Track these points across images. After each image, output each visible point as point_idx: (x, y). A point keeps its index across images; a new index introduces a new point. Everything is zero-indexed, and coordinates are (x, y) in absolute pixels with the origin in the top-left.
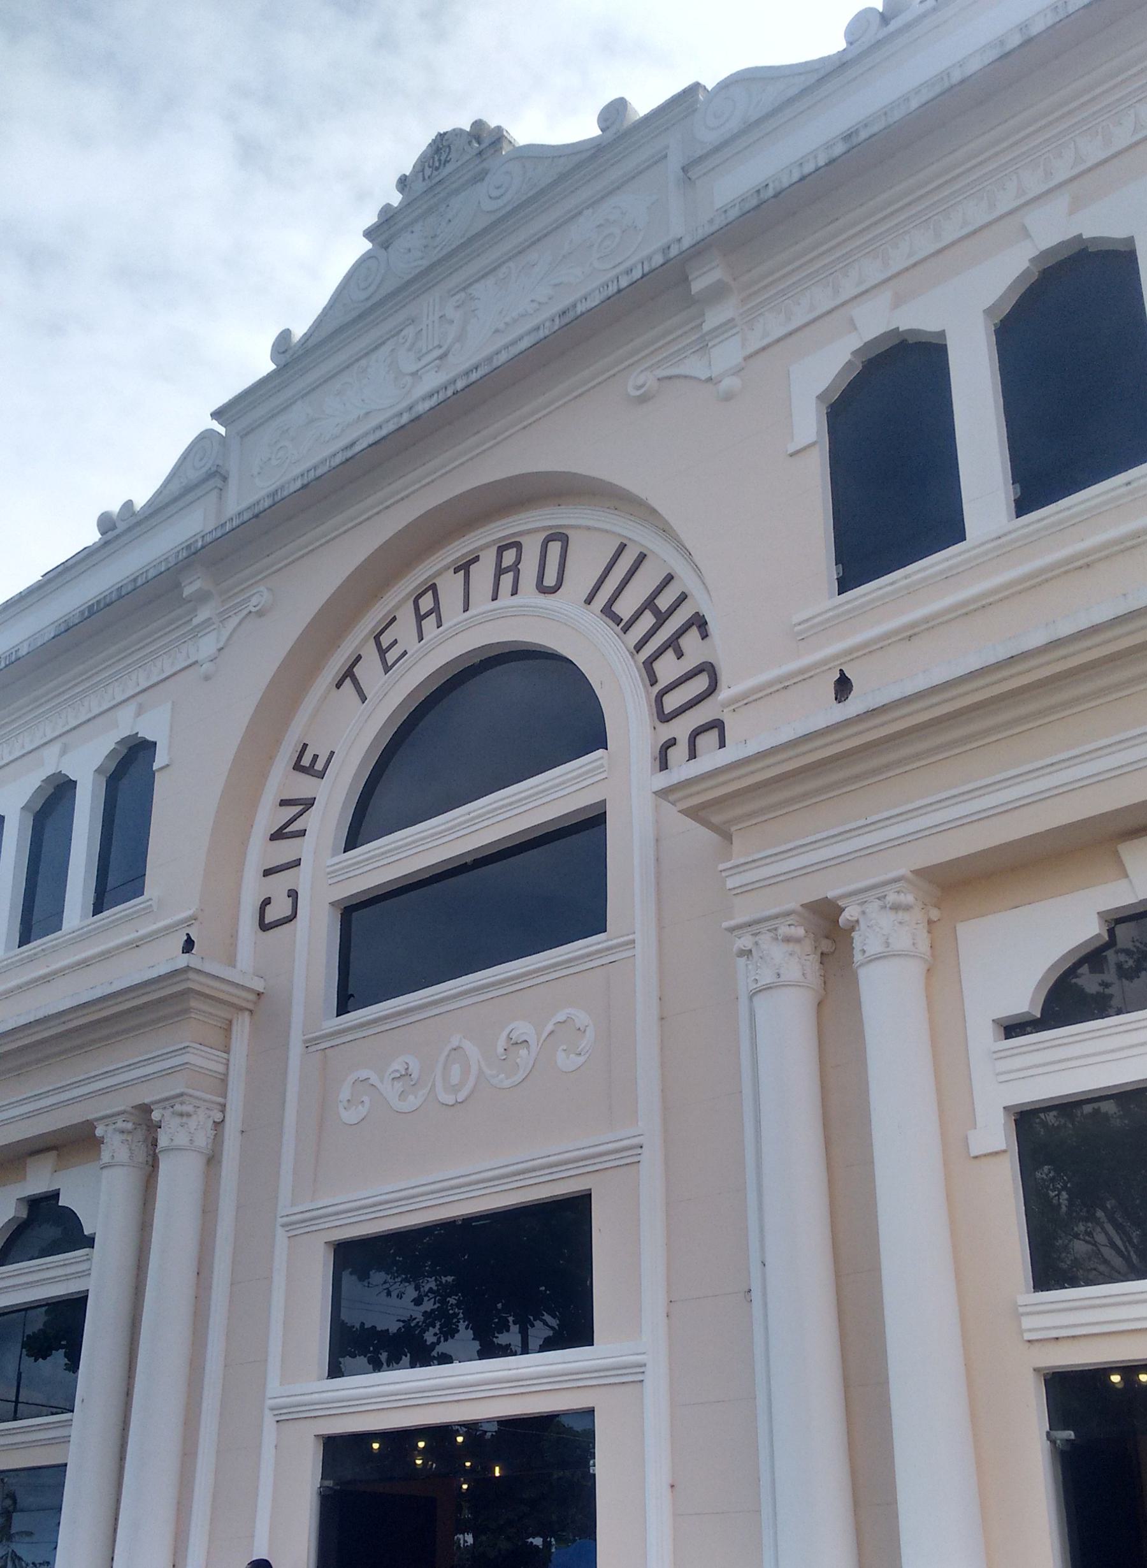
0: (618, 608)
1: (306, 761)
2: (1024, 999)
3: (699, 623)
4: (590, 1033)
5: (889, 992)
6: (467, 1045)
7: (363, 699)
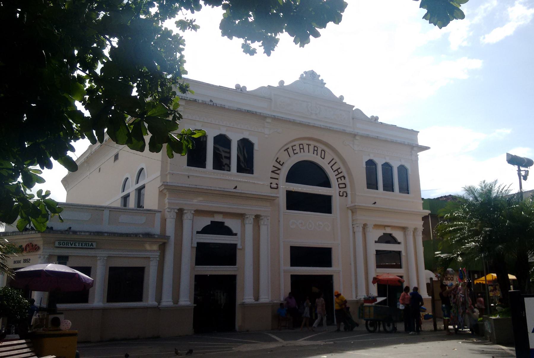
3: (344, 178)
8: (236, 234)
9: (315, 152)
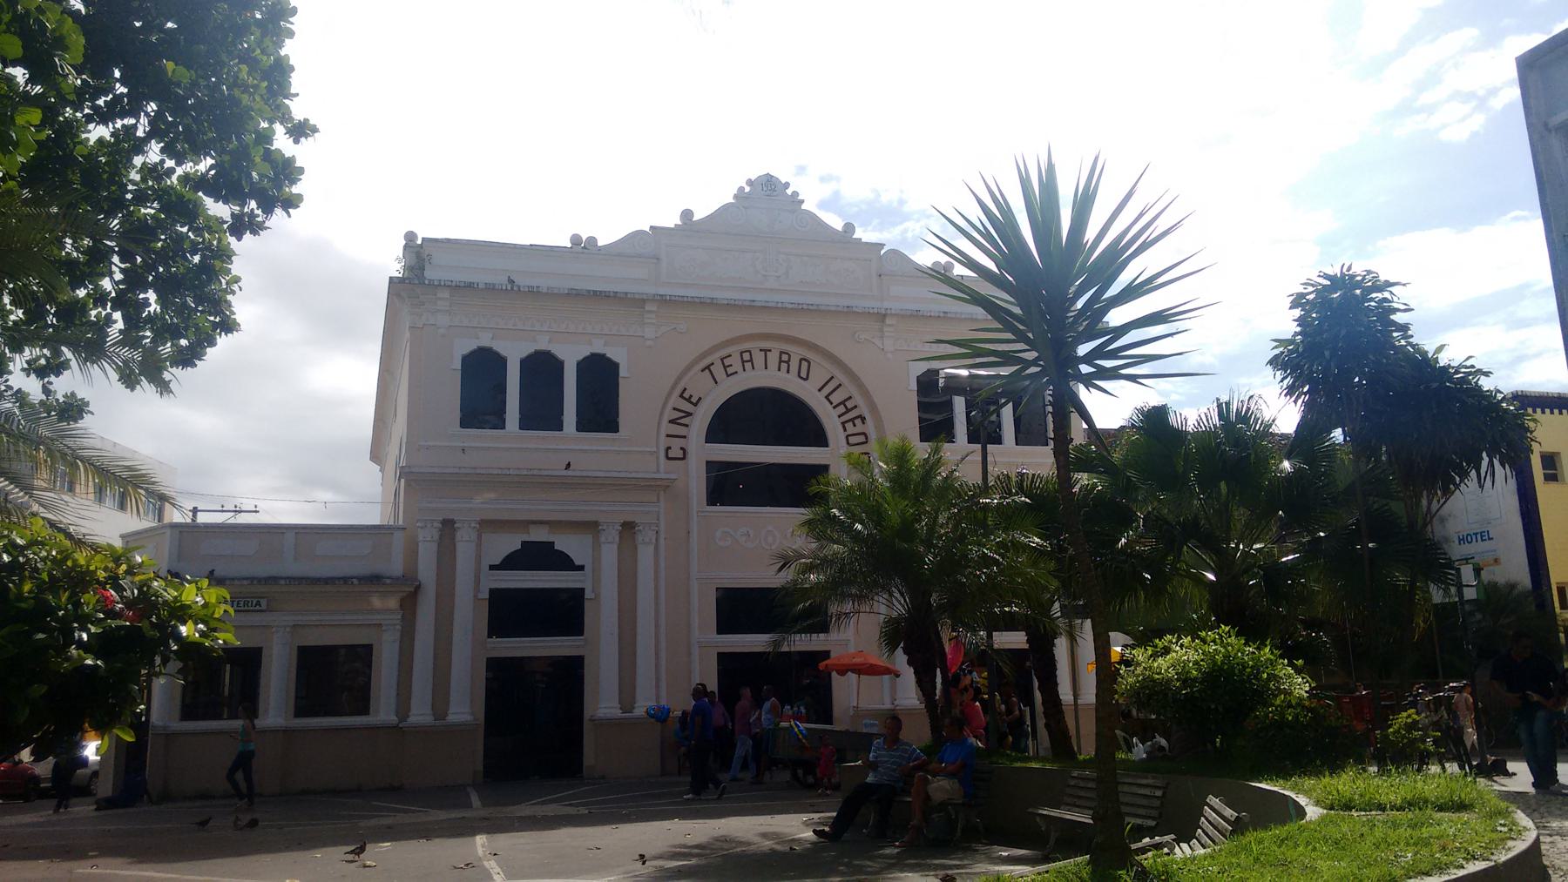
1: (686, 395)
3: (863, 419)
8: (581, 568)
9: (784, 366)
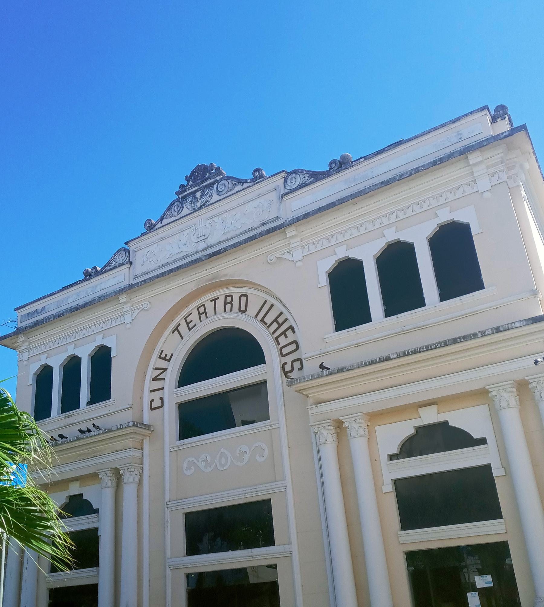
0: (265, 320)
1: (163, 356)
2: (395, 450)
3: (291, 328)
4: (267, 450)
5: (359, 446)
6: (226, 451)
7: (182, 338)
9: (228, 306)
